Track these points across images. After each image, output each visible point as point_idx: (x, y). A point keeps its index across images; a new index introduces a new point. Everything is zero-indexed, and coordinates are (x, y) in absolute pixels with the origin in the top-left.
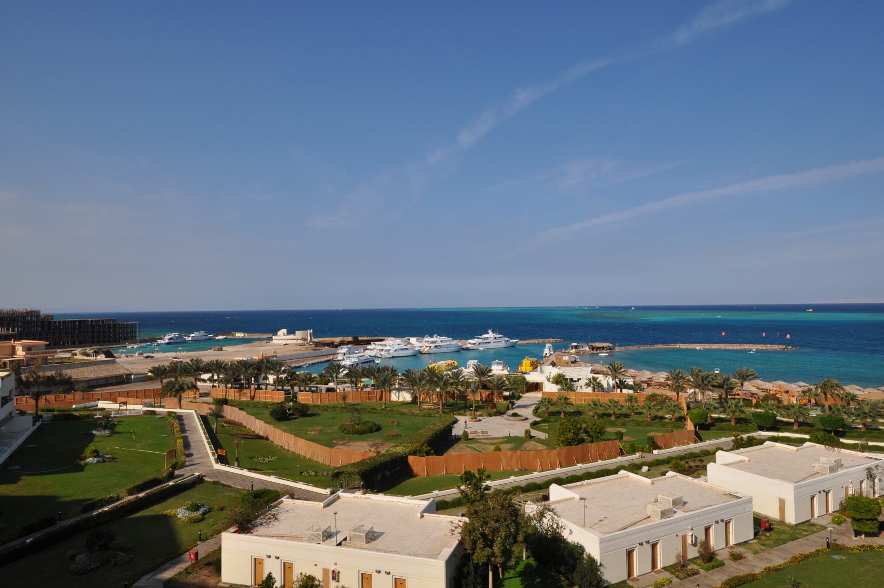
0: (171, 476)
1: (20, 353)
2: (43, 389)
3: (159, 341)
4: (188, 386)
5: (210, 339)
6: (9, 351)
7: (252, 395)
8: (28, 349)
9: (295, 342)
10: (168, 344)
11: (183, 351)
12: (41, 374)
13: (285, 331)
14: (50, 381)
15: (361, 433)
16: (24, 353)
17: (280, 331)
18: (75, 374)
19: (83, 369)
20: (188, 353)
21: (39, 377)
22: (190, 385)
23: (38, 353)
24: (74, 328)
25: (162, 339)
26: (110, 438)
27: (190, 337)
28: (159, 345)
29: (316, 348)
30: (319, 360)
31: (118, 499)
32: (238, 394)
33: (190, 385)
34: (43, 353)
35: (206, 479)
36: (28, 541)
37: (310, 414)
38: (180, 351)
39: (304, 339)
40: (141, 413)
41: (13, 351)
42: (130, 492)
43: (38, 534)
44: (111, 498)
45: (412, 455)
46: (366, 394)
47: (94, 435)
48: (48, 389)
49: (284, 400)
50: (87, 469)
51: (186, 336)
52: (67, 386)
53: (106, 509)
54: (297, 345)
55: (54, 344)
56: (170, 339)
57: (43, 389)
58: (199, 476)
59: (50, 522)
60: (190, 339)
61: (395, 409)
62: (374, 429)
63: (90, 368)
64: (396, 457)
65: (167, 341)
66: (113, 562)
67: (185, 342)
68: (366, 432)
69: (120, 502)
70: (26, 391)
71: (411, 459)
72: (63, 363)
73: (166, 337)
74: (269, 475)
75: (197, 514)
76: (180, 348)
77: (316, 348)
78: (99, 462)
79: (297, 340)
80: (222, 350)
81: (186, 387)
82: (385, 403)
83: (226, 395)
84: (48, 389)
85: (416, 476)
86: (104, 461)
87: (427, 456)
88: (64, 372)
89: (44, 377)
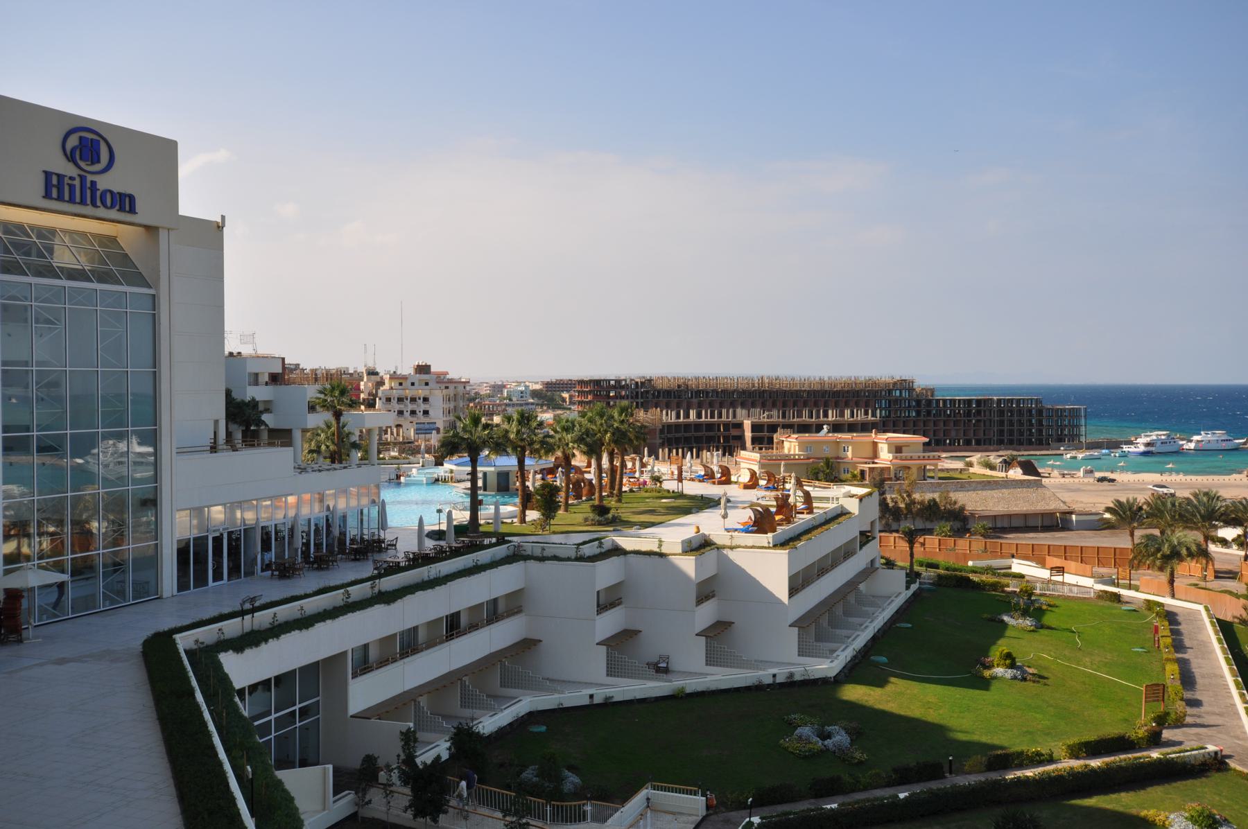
0: (1154, 740)
1: (885, 457)
2: (920, 524)
3: (1126, 448)
4: (1188, 549)
5: (1236, 449)
6: (870, 454)
8: (898, 449)
10: (1145, 454)
11: (1178, 472)
12: (917, 496)
14: (932, 512)
16: (890, 456)
18: (971, 501)
19: (984, 493)
20: (1189, 478)
21: (913, 502)
22: (1194, 548)
23: (911, 459)
24: (968, 414)
25: (1130, 443)
26: (1036, 636)
27: (1191, 441)
28: (1124, 455)
31: (1051, 760)
33: (1194, 548)
34: (919, 458)
35: (1232, 764)
36: (902, 796)
38: (1170, 471)
40: (1092, 595)
41: (875, 455)
42: (1076, 751)
43: (918, 788)
44: (1038, 754)
47: (1005, 625)
48: (929, 525)
50: (995, 686)
51: (1183, 440)
52: (958, 525)
53: (1029, 773)
55: (936, 443)
56: (1148, 445)
57: (920, 524)
58: (1216, 753)
59: (933, 771)
60: (1192, 446)
63: (996, 494)
65: (1142, 448)
67: (1179, 452)
70: (894, 526)
72: (949, 479)
73: (1138, 440)
76: (1170, 466)
78: (1015, 678)
81: (1184, 552)
84: (929, 525)
86: (1024, 679)
88: (954, 496)
89: (922, 503)
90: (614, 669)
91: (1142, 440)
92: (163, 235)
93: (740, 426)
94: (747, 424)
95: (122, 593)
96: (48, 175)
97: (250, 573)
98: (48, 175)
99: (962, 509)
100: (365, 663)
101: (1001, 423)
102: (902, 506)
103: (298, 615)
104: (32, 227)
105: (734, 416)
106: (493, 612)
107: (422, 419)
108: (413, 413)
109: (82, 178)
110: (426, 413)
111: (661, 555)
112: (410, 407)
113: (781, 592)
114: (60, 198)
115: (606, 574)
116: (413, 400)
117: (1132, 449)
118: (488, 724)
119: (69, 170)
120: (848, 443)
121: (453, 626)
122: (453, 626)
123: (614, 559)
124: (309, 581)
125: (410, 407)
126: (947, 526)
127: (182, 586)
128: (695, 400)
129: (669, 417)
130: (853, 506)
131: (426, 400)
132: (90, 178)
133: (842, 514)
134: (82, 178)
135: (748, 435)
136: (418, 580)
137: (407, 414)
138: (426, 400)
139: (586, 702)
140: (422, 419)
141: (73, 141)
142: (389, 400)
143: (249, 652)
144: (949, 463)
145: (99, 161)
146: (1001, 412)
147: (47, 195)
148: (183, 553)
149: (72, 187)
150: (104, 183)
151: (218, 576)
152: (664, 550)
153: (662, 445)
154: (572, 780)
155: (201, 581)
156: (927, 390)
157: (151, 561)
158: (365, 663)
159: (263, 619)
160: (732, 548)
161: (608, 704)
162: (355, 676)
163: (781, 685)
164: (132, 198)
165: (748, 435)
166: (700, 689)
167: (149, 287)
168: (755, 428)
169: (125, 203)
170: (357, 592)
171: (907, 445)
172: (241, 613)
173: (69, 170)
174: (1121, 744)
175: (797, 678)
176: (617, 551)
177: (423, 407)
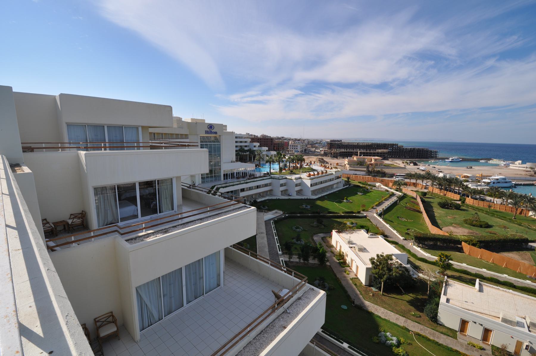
0: (359, 212)
1: (373, 162)
3: (446, 160)
4: (402, 184)
6: (370, 161)
7: (445, 193)
8: (376, 160)
9: (525, 169)
10: (451, 162)
11: (450, 166)
12: (375, 169)
13: (520, 162)
14: (378, 172)
15: (474, 226)
17: (517, 162)
18: (387, 171)
20: (453, 168)
21: (374, 170)
23: (378, 162)
24: (410, 151)
25: (448, 159)
26: (361, 196)
29: (534, 175)
30: (523, 183)
31: (339, 213)
32: (439, 192)
34: (380, 162)
35: (367, 217)
37: (461, 209)
38: (449, 166)
39: (532, 168)
43: (311, 215)
45: (464, 242)
46: (510, 208)
47: (357, 194)
48: (377, 175)
49: (459, 199)
50: (343, 203)
52: (383, 175)
53: (331, 215)
54: (524, 171)
61: (518, 221)
62: (483, 226)
64: (452, 239)
65: (450, 160)
66: (319, 227)
68: (477, 226)
69: (337, 214)
71: (463, 243)
72: (388, 166)
74: (387, 223)
75: (351, 225)
77: (534, 175)
78: (346, 202)
79: (527, 168)
80: (471, 168)
81: (401, 184)
82: (515, 216)
83: (433, 190)
84: (377, 175)
85: (464, 253)
87: (471, 245)
88: (383, 170)
90: (282, 195)
91: (451, 159)
92: (221, 136)
93: (358, 152)
94: (359, 152)
95: (216, 180)
96: (206, 131)
97: (234, 178)
98: (206, 131)
99: (385, 172)
100: (243, 190)
101: (418, 153)
102: (372, 171)
103: (233, 184)
104: (205, 136)
105: (357, 150)
106: (266, 185)
107: (296, 150)
108: (295, 148)
109: (210, 131)
110: (297, 148)
111: (291, 179)
112: (294, 147)
113: (309, 186)
114: (207, 133)
115: (282, 182)
116: (295, 146)
117: (448, 160)
118: (259, 200)
119: (209, 130)
120: (366, 158)
121: (258, 187)
122: (258, 187)
123: (286, 179)
124: (241, 179)
125: (294, 147)
126: (381, 175)
127: (224, 179)
128: (350, 147)
129: (343, 150)
130: (334, 173)
131: (297, 146)
132: (211, 131)
133: (332, 174)
134: (210, 131)
135: (359, 154)
136: (253, 181)
137: (294, 148)
138: (297, 146)
139: (276, 199)
140: (296, 150)
141: (209, 126)
142: (291, 146)
143: (227, 188)
144: (386, 162)
145: (212, 128)
146: (418, 151)
147: (206, 133)
148: (224, 175)
149: (209, 132)
150: (213, 131)
151: (229, 178)
152: (292, 179)
153: (339, 156)
154: (267, 207)
155: (227, 179)
156: (401, 146)
157: (220, 176)
158: (243, 190)
159: (228, 185)
160: (303, 179)
161: (279, 199)
162: (241, 192)
163: (306, 199)
164: (217, 132)
165: (359, 154)
166: (293, 198)
167: (219, 142)
168: (360, 153)
169: (216, 133)
170: (242, 182)
171: (378, 159)
172: (225, 184)
173: (209, 130)
174: (353, 213)
175: (308, 198)
176: (286, 178)
177: (296, 147)
